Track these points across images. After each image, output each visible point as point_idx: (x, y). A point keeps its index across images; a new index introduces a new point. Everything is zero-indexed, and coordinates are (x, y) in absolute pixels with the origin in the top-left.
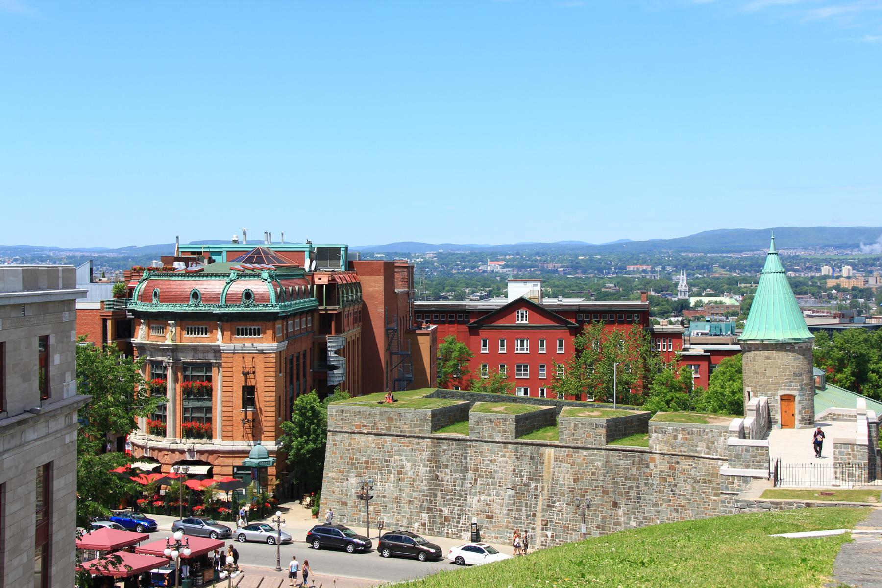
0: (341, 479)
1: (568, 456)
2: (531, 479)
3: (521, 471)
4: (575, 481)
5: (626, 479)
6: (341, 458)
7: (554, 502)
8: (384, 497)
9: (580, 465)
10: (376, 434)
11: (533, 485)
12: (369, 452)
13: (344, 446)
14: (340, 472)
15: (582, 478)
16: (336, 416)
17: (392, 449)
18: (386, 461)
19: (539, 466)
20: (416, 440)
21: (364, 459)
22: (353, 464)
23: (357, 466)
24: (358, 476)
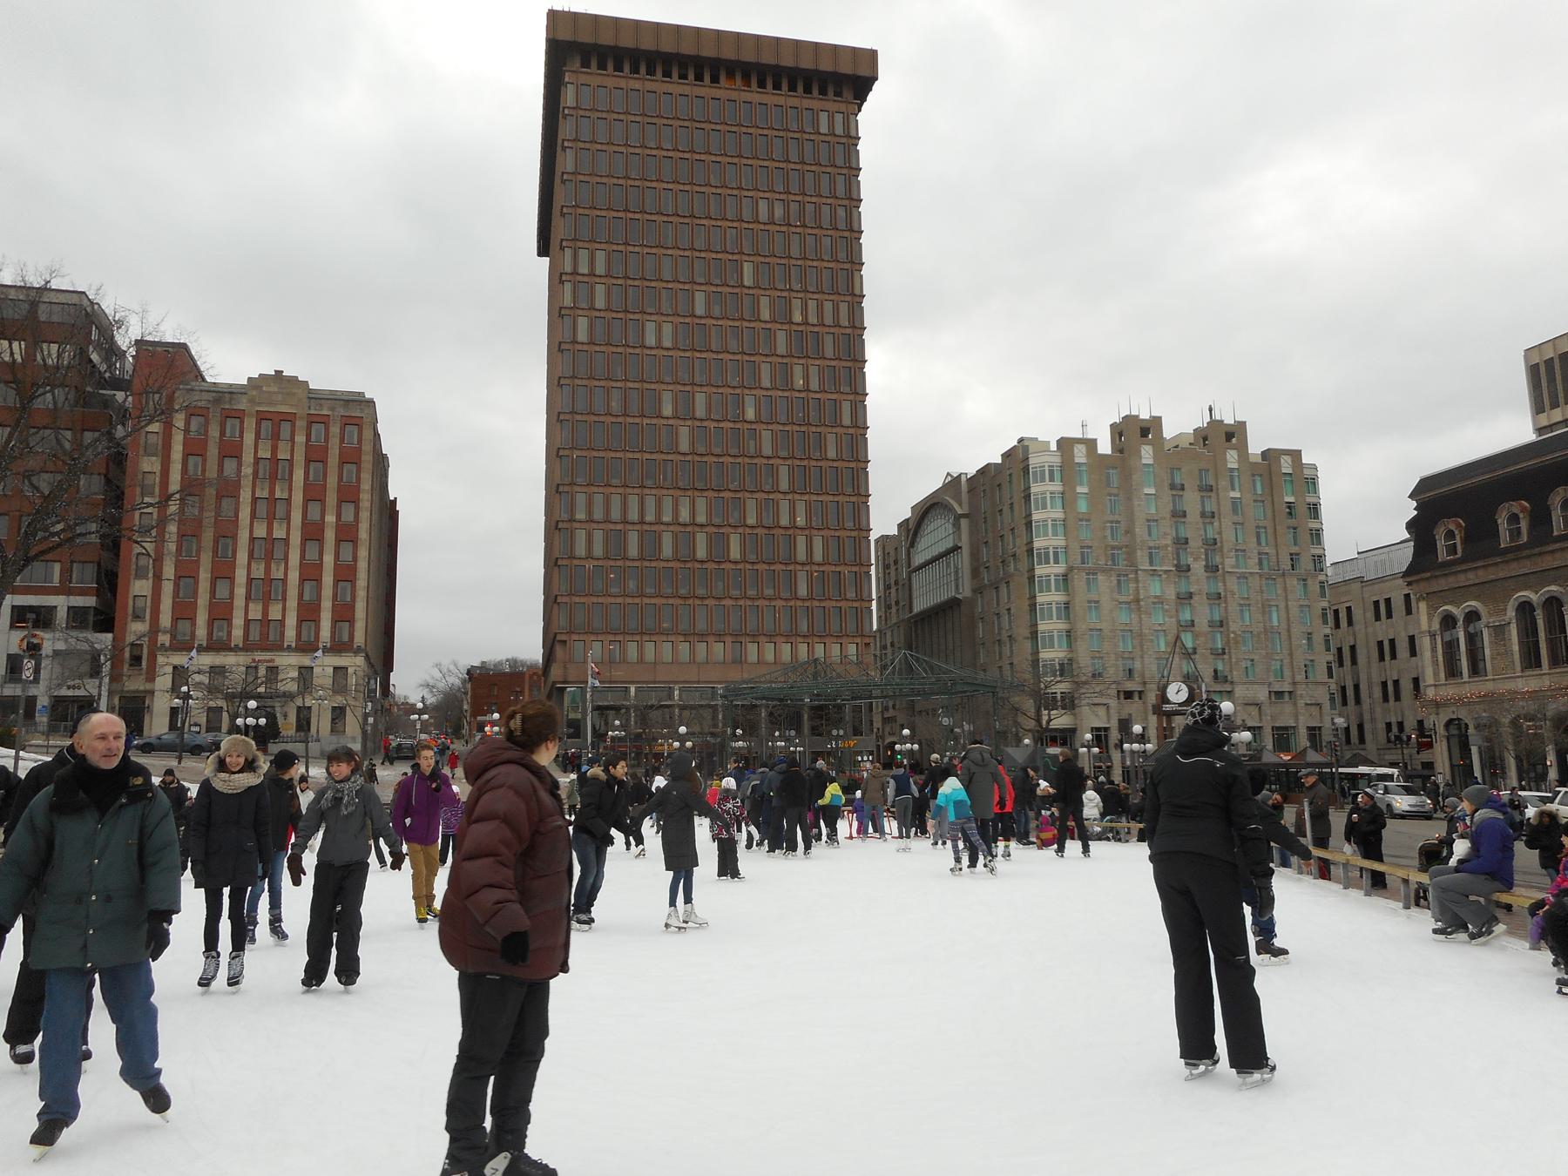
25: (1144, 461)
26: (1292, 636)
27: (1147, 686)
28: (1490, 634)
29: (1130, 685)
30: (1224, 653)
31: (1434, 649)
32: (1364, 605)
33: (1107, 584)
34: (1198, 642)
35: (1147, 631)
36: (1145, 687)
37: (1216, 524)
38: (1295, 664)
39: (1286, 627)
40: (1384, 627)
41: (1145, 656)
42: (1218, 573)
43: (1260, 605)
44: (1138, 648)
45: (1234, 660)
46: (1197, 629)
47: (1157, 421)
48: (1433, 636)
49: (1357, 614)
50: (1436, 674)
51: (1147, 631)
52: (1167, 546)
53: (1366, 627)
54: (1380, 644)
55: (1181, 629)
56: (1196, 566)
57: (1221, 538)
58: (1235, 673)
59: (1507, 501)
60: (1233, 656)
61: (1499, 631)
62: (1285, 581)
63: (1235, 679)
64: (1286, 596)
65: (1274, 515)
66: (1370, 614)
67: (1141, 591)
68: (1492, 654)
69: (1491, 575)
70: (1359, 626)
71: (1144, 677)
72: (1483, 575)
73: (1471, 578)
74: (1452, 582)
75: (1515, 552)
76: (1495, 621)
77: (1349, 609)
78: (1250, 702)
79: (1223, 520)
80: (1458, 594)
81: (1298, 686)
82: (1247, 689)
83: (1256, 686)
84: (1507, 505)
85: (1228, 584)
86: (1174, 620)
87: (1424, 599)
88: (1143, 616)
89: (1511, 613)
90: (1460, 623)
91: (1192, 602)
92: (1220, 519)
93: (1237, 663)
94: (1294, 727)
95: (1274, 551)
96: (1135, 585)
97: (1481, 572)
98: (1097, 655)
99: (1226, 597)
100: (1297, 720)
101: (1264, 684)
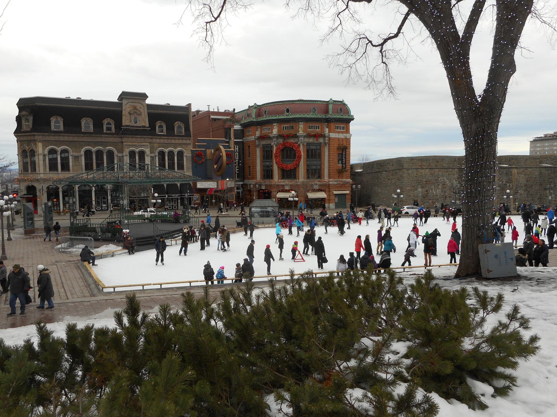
0: (414, 190)
1: (523, 171)
2: (507, 182)
3: (502, 179)
4: (527, 181)
5: (549, 179)
6: (413, 180)
7: (518, 191)
8: (437, 196)
9: (528, 175)
10: (430, 169)
11: (508, 185)
12: (427, 177)
13: (414, 175)
14: (413, 187)
15: (530, 180)
16: (409, 162)
17: (439, 175)
18: (436, 180)
19: (510, 177)
20: (451, 170)
21: (425, 180)
22: (419, 182)
23: (421, 183)
24: (422, 187)
28: (72, 159)
31: (44, 160)
48: (44, 156)
50: (45, 169)
59: (87, 117)
61: (76, 158)
68: (73, 165)
69: (76, 139)
72: (71, 139)
73: (66, 138)
74: (57, 138)
75: (86, 134)
76: (76, 154)
80: (59, 143)
84: (87, 119)
87: (41, 142)
89: (82, 153)
90: (59, 153)
97: (71, 138)
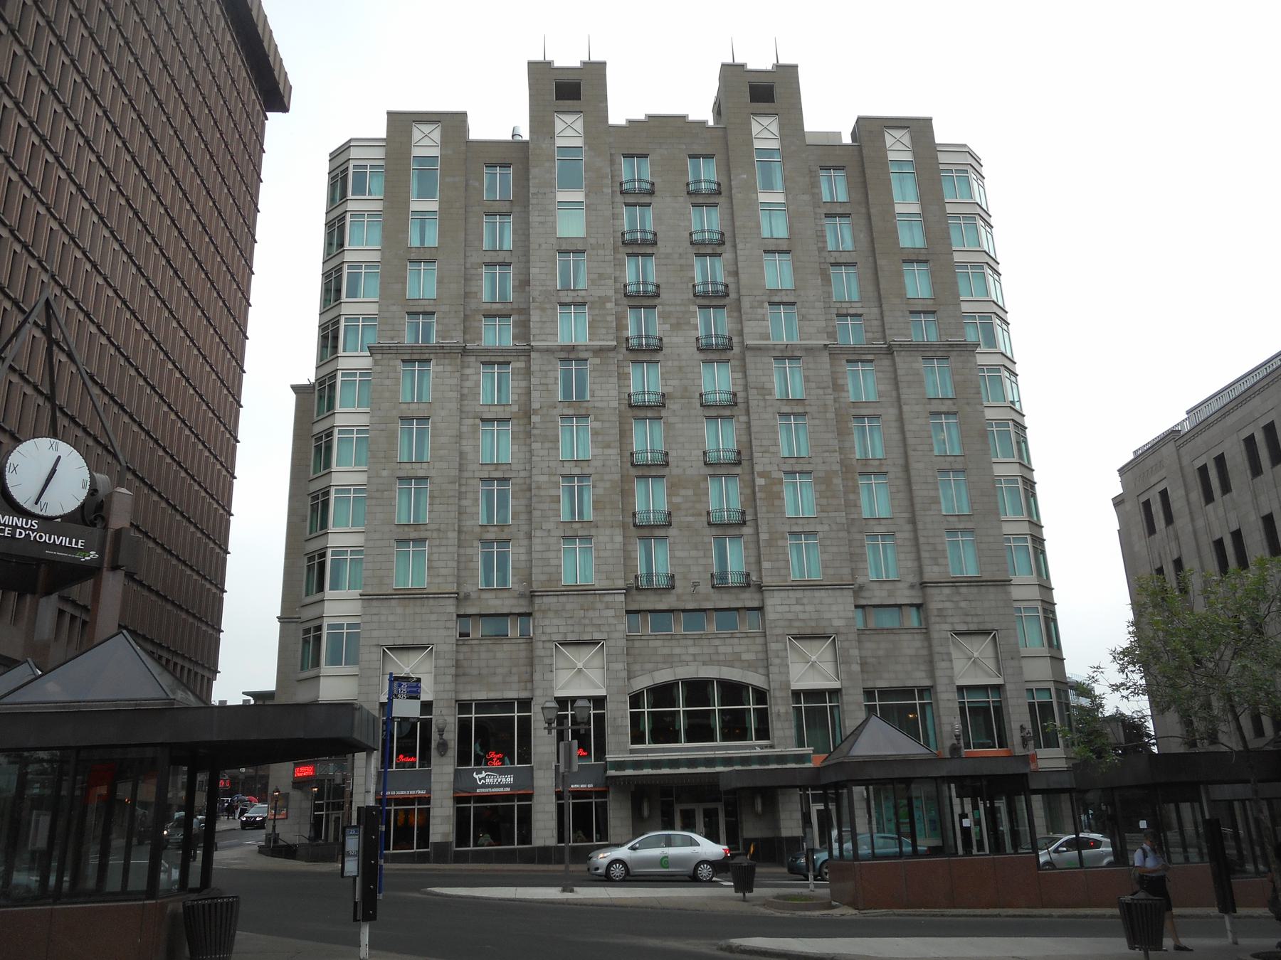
25: (560, 142)
26: (914, 479)
27: (537, 601)
29: (498, 602)
30: (744, 523)
32: (1184, 481)
33: (454, 381)
34: (676, 500)
35: (544, 478)
36: (532, 603)
37: (728, 255)
38: (922, 540)
39: (901, 462)
40: (1221, 511)
41: (538, 533)
42: (730, 354)
43: (831, 415)
44: (523, 517)
45: (763, 536)
46: (674, 470)
47: (595, 71)
49: (1177, 504)
51: (544, 478)
52: (603, 300)
53: (1193, 520)
54: (1219, 544)
55: (633, 472)
56: (675, 340)
57: (738, 282)
58: (766, 565)
60: (763, 528)
62: (894, 364)
63: (767, 580)
64: (899, 398)
65: (872, 241)
66: (1196, 495)
67: (535, 395)
70: (1182, 521)
71: (529, 579)
77: (1164, 494)
78: (808, 631)
79: (740, 246)
81: (930, 591)
82: (798, 602)
83: (823, 593)
85: (750, 372)
86: (613, 452)
88: (535, 446)
91: (664, 413)
92: (735, 246)
93: (770, 542)
94: (923, 691)
95: (876, 311)
96: (523, 384)
98: (413, 535)
99: (747, 402)
100: (932, 673)
101: (840, 587)
